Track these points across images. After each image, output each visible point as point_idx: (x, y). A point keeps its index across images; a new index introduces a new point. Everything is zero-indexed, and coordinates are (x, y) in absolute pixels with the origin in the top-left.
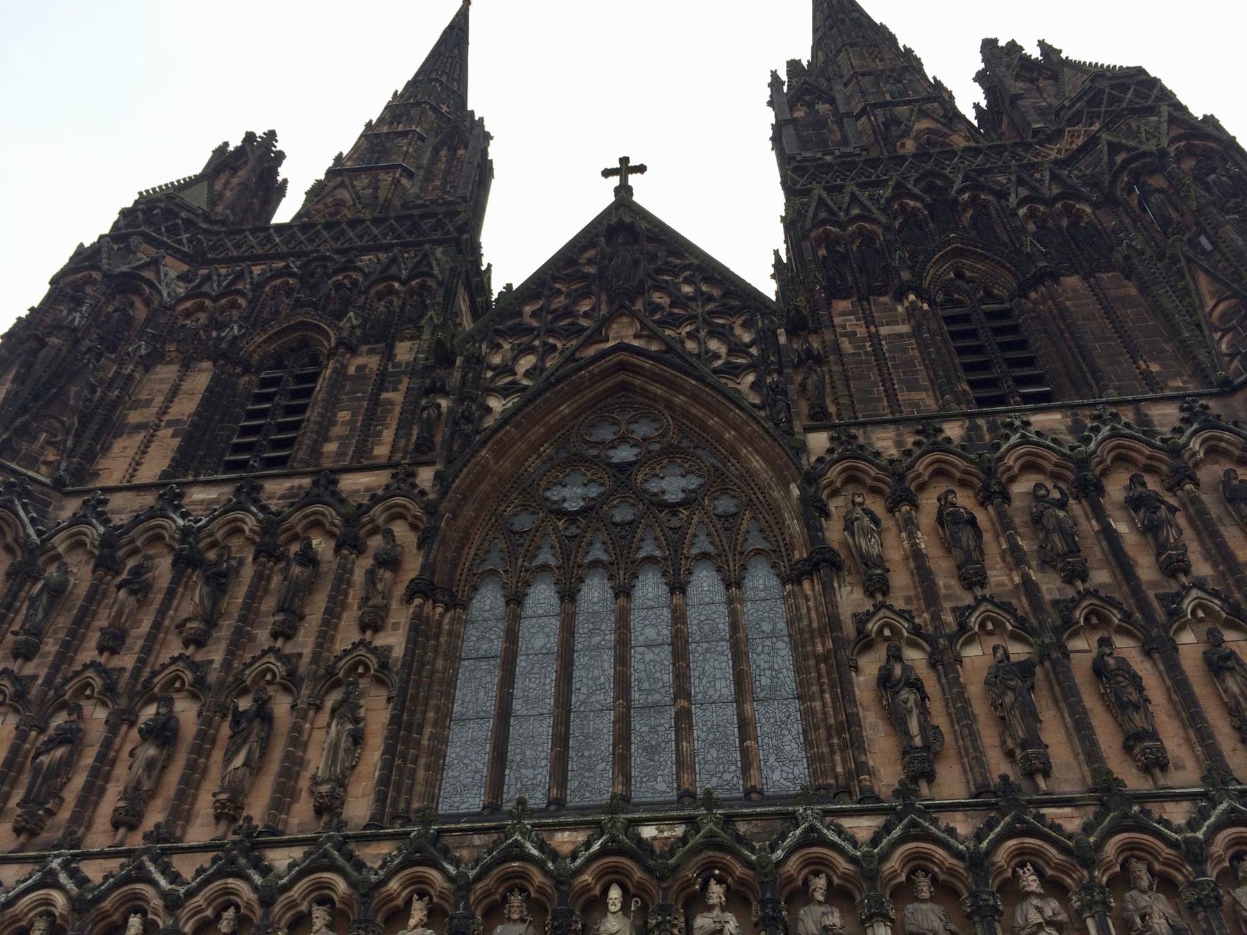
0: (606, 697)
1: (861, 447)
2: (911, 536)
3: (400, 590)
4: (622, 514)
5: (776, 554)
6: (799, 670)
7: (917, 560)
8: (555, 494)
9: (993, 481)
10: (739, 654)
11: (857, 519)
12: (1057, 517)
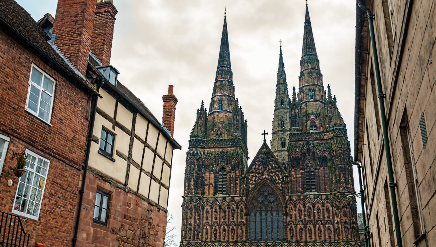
0: (265, 227)
1: (292, 199)
2: (295, 212)
3: (244, 214)
4: (266, 203)
5: (283, 211)
6: (283, 226)
7: (295, 214)
8: (259, 199)
10: (277, 224)
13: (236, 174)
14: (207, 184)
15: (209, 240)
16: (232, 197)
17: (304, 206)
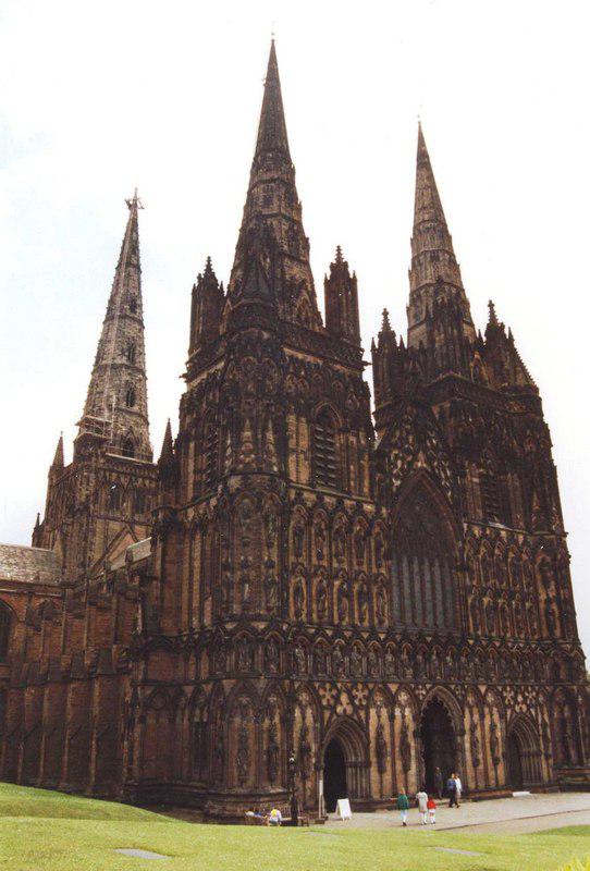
13: (358, 441)
14: (293, 450)
15: (304, 617)
16: (358, 501)
17: (492, 554)
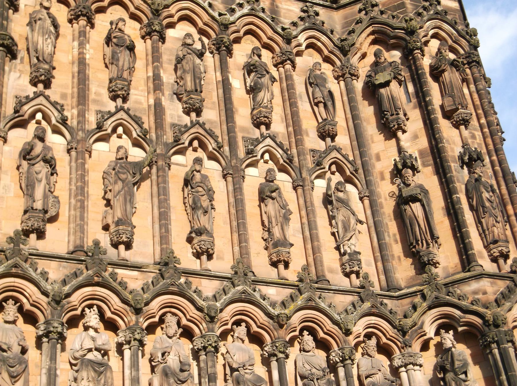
2: (81, 45)
9: (156, 22)
11: (40, 19)
12: (194, 63)
